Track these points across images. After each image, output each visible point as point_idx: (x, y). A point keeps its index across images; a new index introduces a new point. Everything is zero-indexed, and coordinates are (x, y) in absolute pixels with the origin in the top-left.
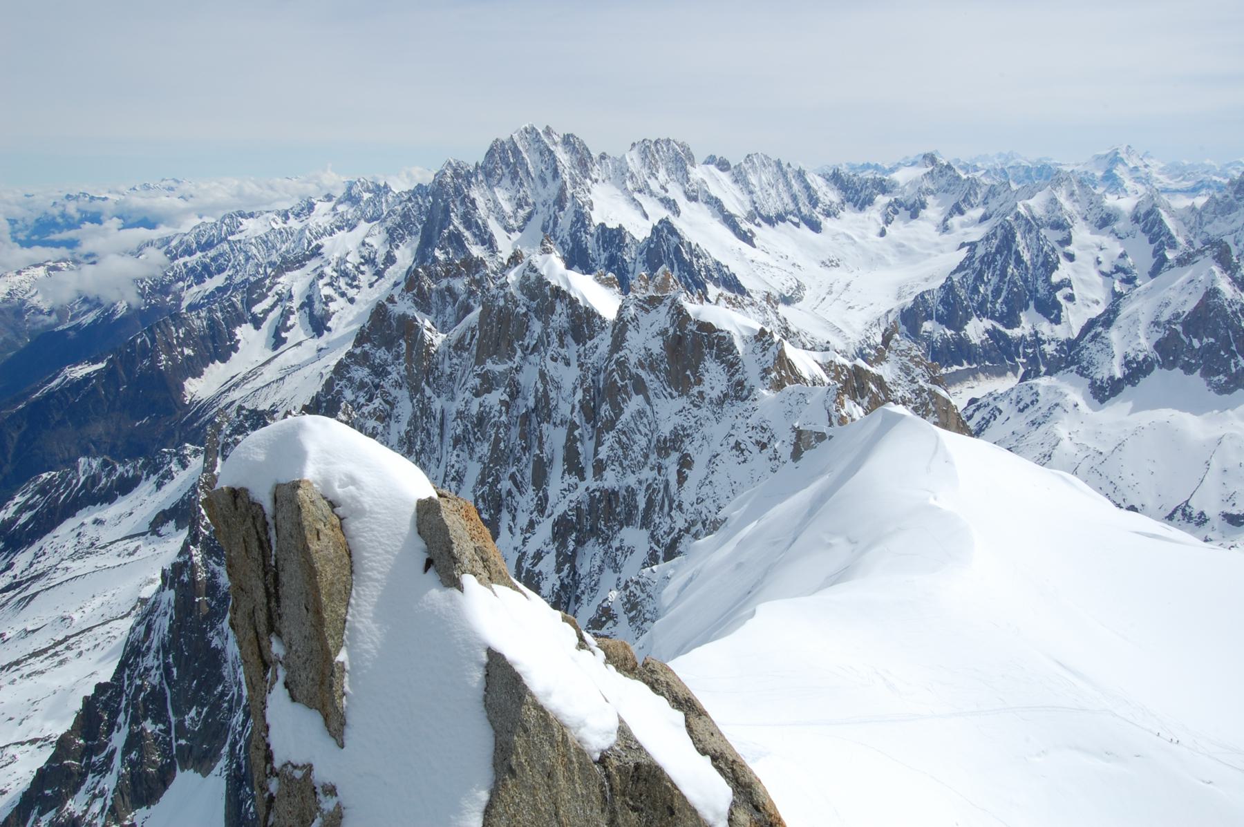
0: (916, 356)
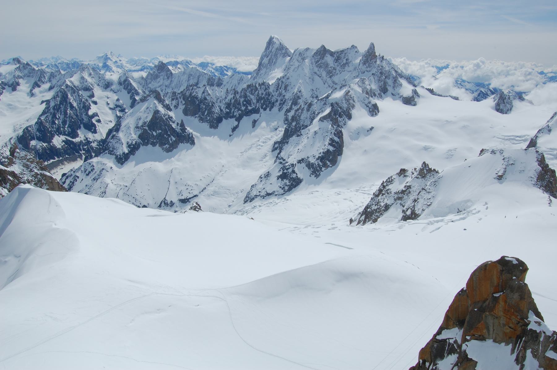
0: (30, 159)
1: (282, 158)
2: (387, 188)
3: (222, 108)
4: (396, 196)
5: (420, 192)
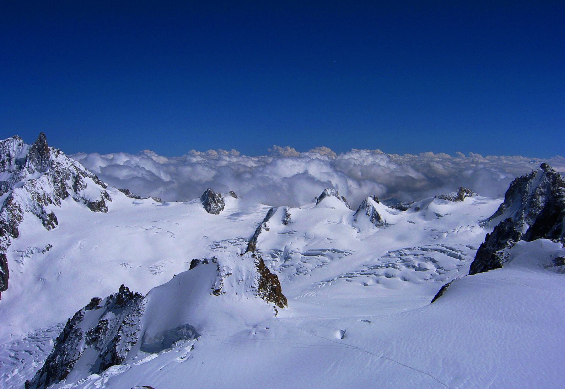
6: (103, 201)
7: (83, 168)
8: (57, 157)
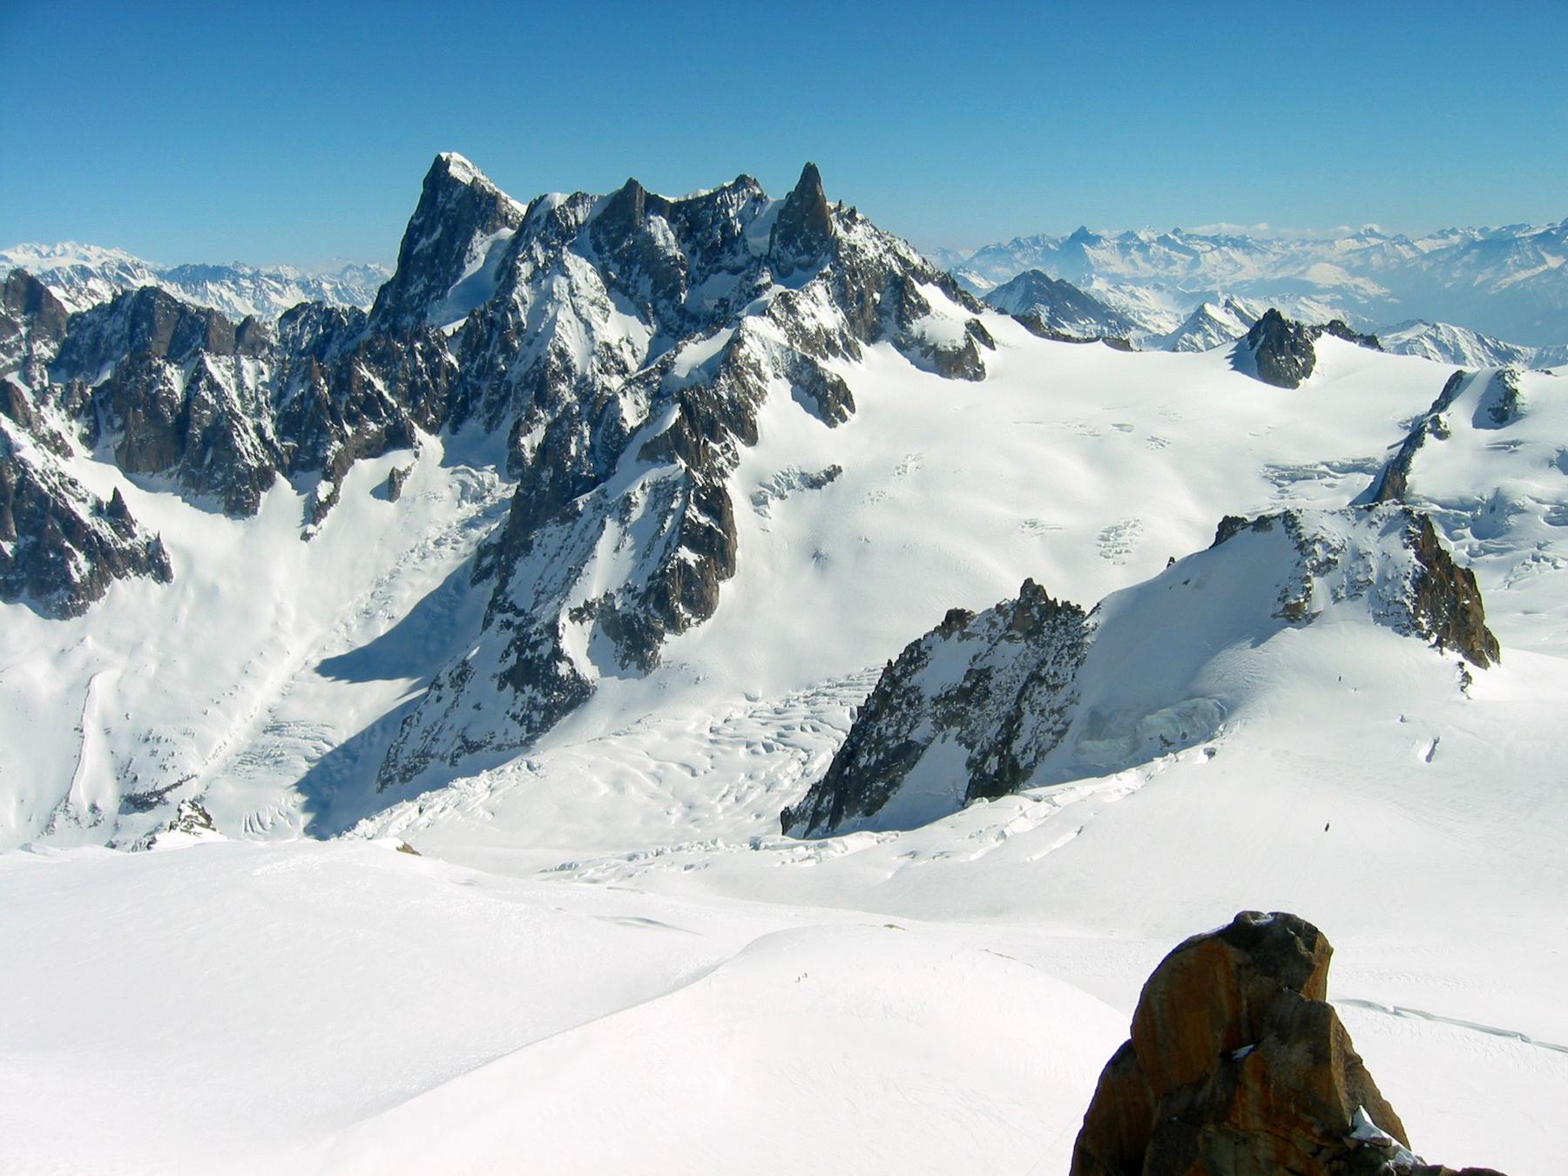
1: (513, 607)
2: (906, 683)
3: (269, 433)
4: (940, 710)
5: (1025, 687)
6: (970, 347)
7: (916, 260)
8: (847, 228)
